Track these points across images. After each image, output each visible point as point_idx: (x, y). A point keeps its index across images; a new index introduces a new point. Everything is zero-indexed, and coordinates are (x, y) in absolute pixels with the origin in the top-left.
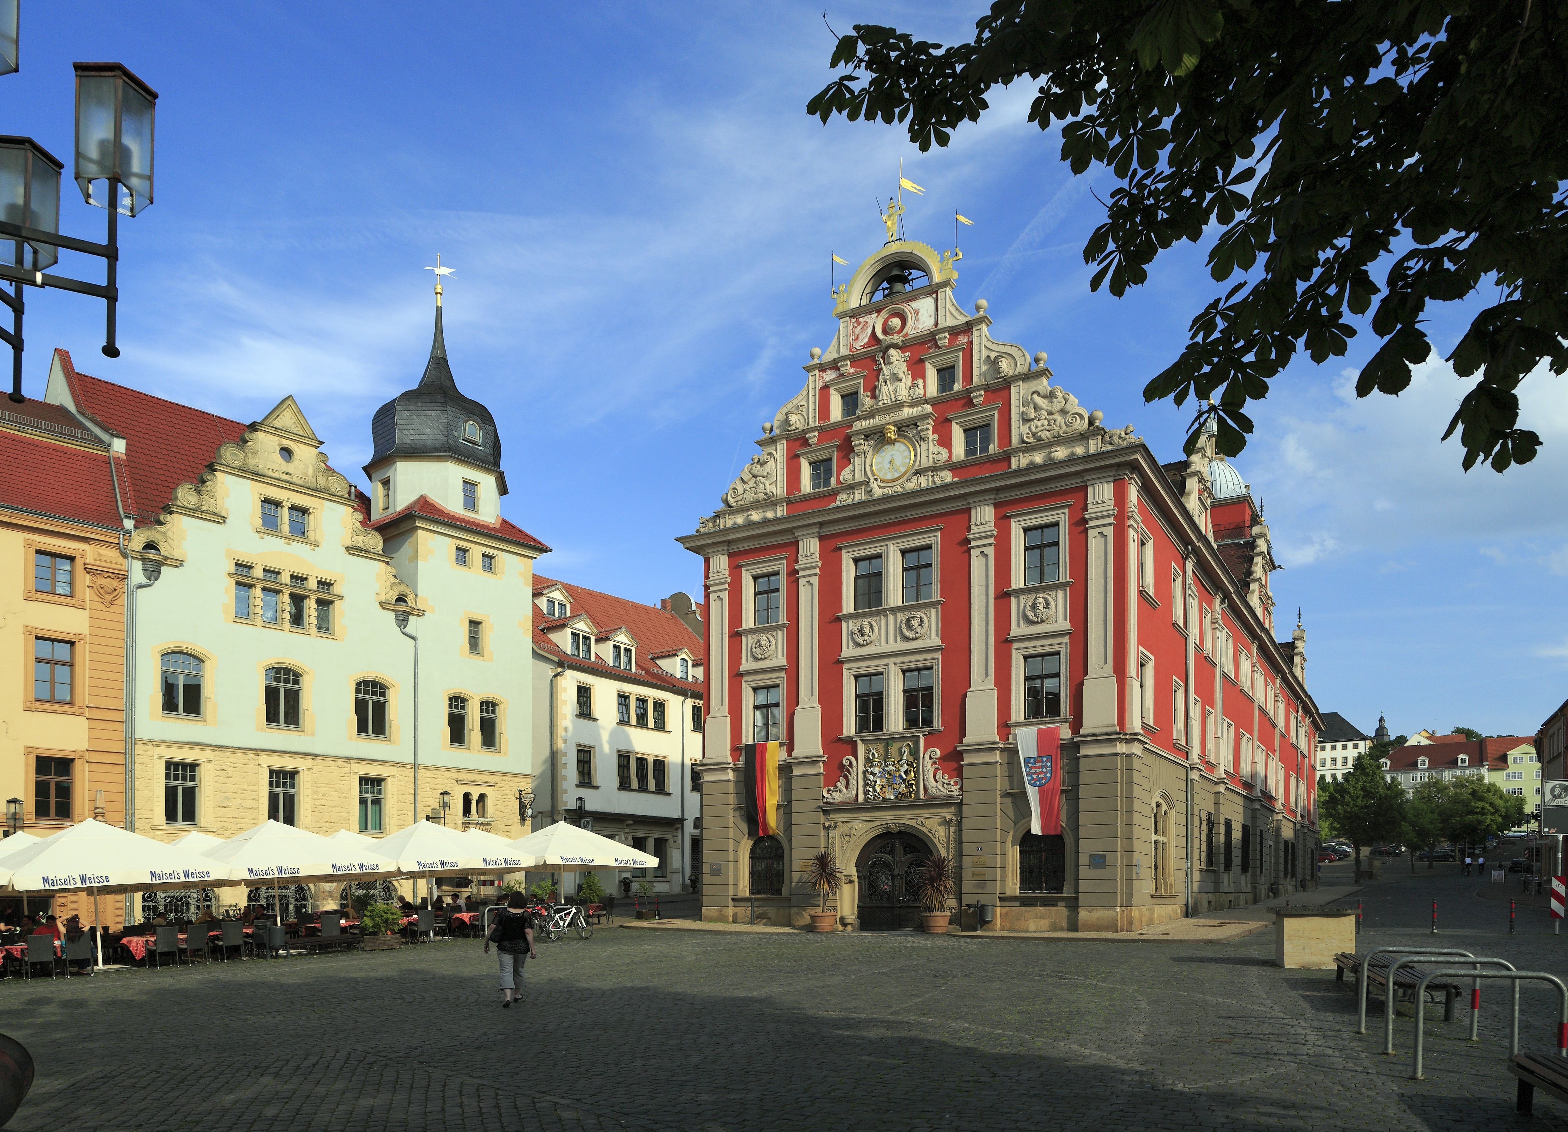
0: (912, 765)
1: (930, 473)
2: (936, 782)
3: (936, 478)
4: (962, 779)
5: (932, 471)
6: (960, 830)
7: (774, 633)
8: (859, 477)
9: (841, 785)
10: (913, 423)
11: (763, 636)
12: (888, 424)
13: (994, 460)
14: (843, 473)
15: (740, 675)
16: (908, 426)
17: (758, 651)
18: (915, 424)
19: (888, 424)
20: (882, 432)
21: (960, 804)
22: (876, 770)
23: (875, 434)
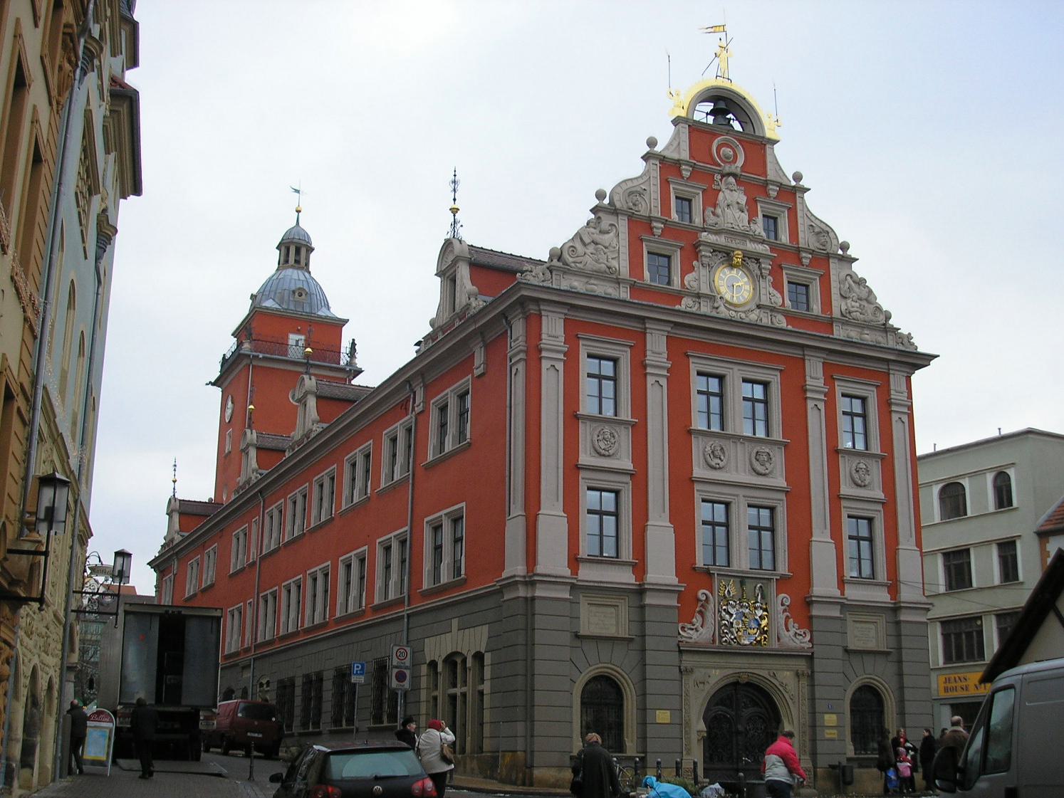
0: (765, 610)
1: (768, 311)
2: (788, 630)
3: (773, 318)
4: (811, 632)
5: (771, 311)
6: (812, 686)
7: (617, 429)
8: (705, 290)
9: (697, 620)
10: (757, 258)
11: (607, 429)
12: (738, 249)
13: (815, 321)
14: (687, 278)
15: (578, 468)
16: (749, 258)
17: (602, 445)
18: (757, 260)
19: (738, 249)
20: (728, 254)
21: (811, 658)
22: (732, 611)
23: (720, 252)
